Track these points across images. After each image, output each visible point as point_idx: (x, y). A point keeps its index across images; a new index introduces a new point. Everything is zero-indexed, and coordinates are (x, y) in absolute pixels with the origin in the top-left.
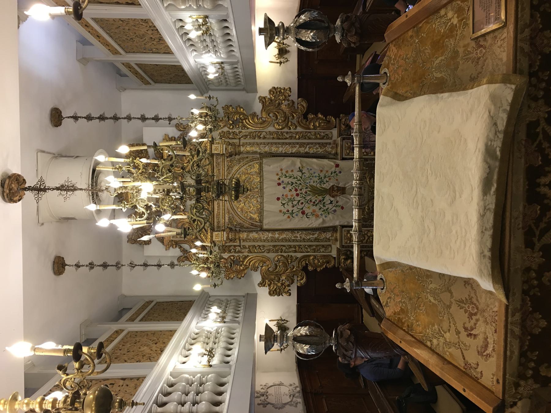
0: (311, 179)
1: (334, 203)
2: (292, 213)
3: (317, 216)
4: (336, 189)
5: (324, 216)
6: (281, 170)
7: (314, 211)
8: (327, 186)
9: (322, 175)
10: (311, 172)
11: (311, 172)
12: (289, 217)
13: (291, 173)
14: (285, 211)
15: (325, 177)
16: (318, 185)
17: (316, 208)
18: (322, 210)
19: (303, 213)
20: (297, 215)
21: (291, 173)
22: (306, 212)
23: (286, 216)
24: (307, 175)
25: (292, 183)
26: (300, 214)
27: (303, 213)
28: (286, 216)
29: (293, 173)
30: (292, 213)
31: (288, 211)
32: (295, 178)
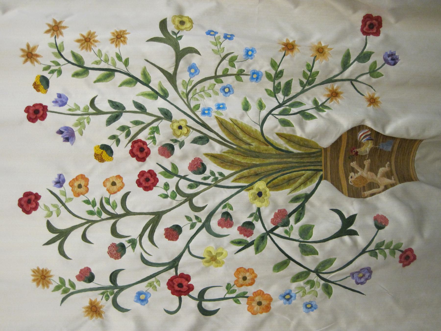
0: (227, 91)
1: (364, 226)
2: (114, 288)
3: (261, 303)
4: (367, 147)
5: (298, 302)
6: (56, 28)
7: (245, 276)
8: (328, 124)
9: (293, 67)
10: (227, 46)
11: (227, 46)
12: (94, 310)
13: (110, 50)
14: (70, 272)
15: (309, 80)
16: (271, 122)
17: (261, 261)
18: (296, 269)
19: (180, 286)
20: (142, 298)
21: (110, 50)
22: (197, 283)
23: (81, 301)
24: (207, 63)
25: (118, 109)
26: (163, 296)
27: (180, 286)
28: (81, 301)
29: (124, 50)
30: (114, 288)
31: (87, 276)
32: (133, 80)
